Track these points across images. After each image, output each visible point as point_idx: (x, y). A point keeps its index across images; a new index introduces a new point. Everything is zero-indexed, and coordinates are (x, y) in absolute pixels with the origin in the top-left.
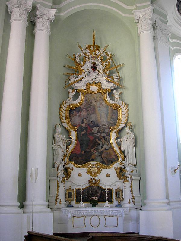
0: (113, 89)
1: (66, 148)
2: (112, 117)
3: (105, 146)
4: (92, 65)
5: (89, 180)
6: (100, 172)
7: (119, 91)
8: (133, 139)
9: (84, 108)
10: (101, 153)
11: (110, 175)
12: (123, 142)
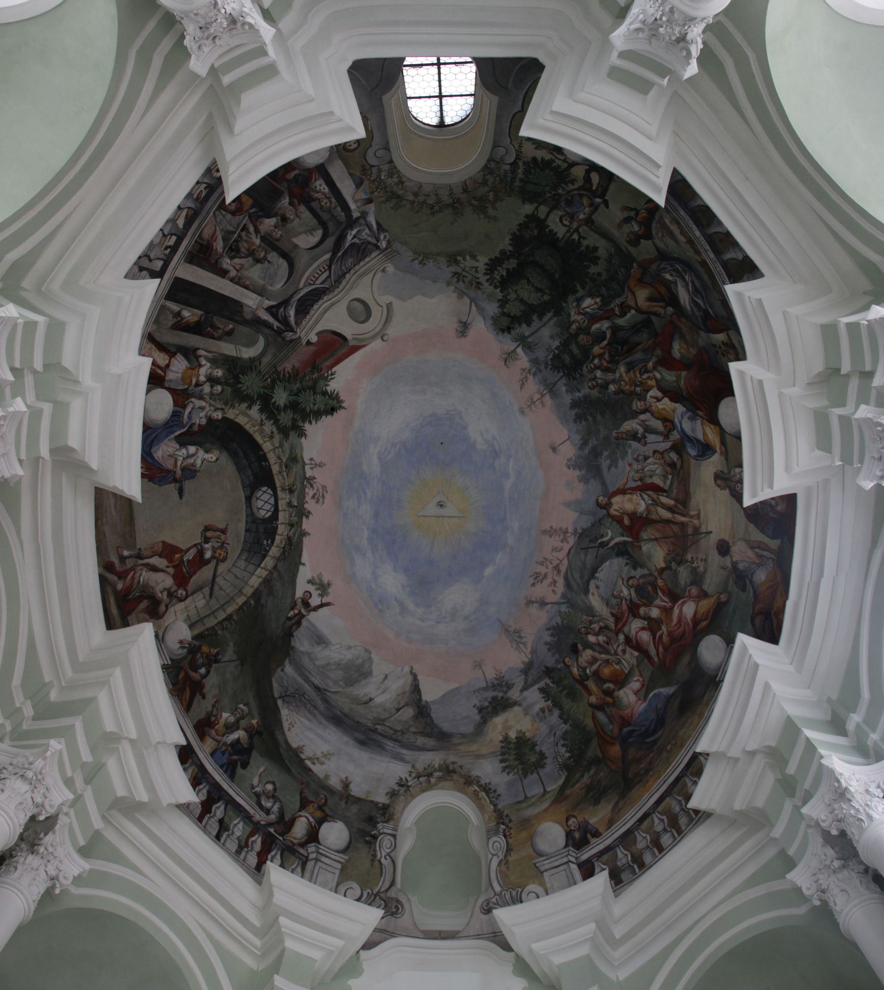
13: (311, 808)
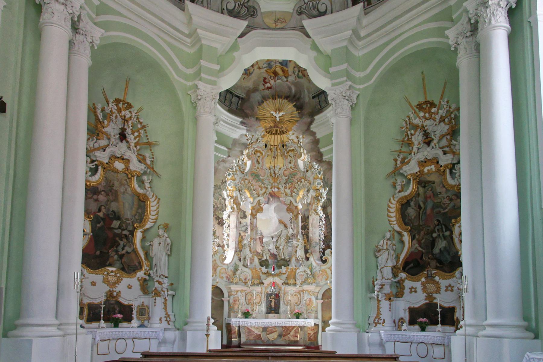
2: (138, 211)
3: (128, 249)
6: (120, 283)
8: (168, 244)
9: (103, 191)
10: (121, 257)
11: (132, 287)
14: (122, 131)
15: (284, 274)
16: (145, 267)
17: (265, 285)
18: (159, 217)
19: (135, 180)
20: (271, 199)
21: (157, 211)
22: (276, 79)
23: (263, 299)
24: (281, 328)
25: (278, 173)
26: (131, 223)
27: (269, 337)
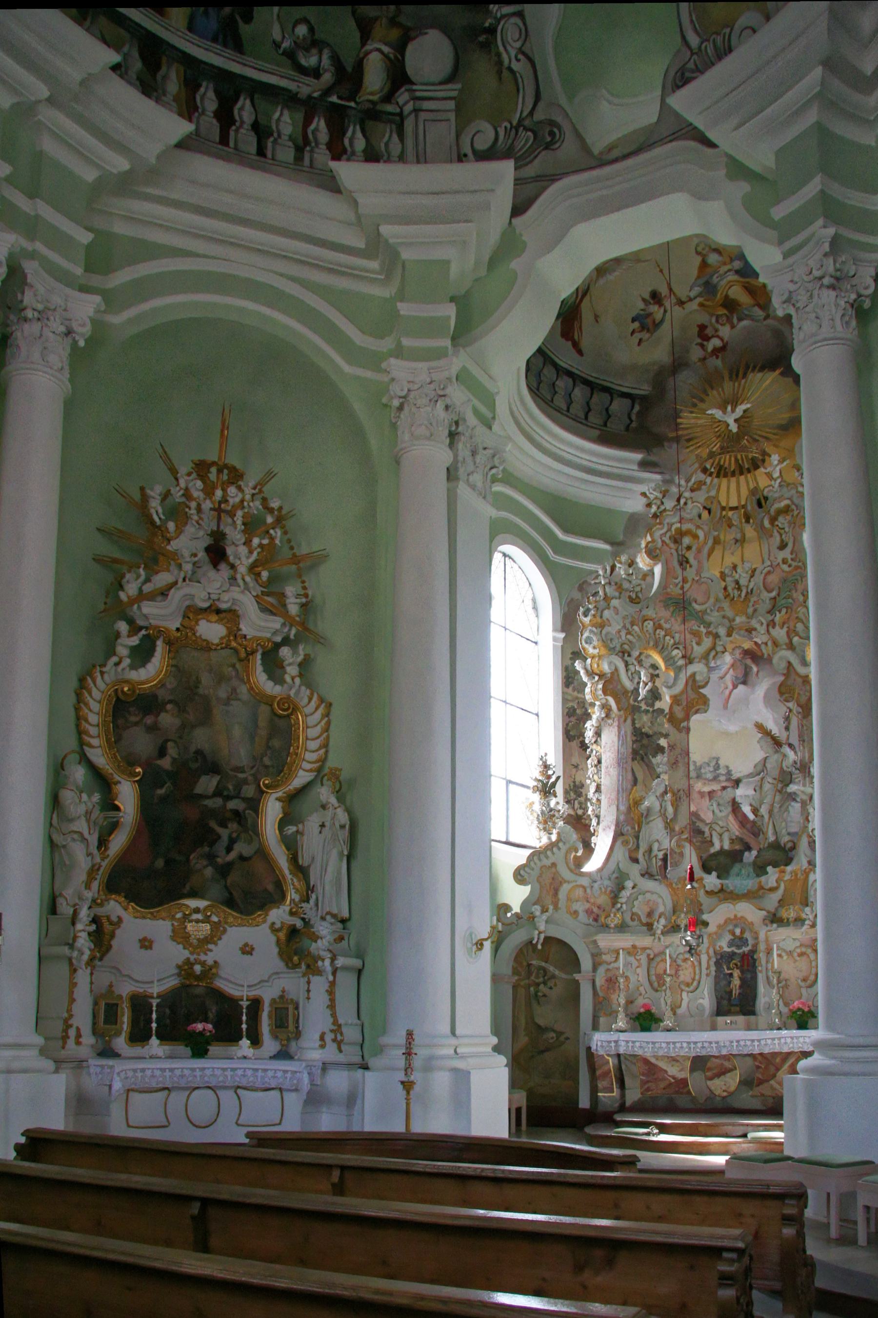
0: (278, 639)
1: (96, 844)
3: (241, 848)
4: (208, 541)
5: (180, 963)
6: (220, 939)
7: (302, 653)
8: (342, 827)
9: (170, 702)
10: (224, 871)
11: (253, 949)
12: (305, 837)
13: (379, 30)
14: (214, 540)
15: (773, 890)
16: (292, 895)
17: (712, 928)
18: (331, 756)
19: (259, 662)
20: (755, 669)
21: (322, 738)
22: (735, 321)
23: (704, 971)
24: (749, 1061)
25: (747, 587)
26: (250, 778)
27: (713, 1088)
